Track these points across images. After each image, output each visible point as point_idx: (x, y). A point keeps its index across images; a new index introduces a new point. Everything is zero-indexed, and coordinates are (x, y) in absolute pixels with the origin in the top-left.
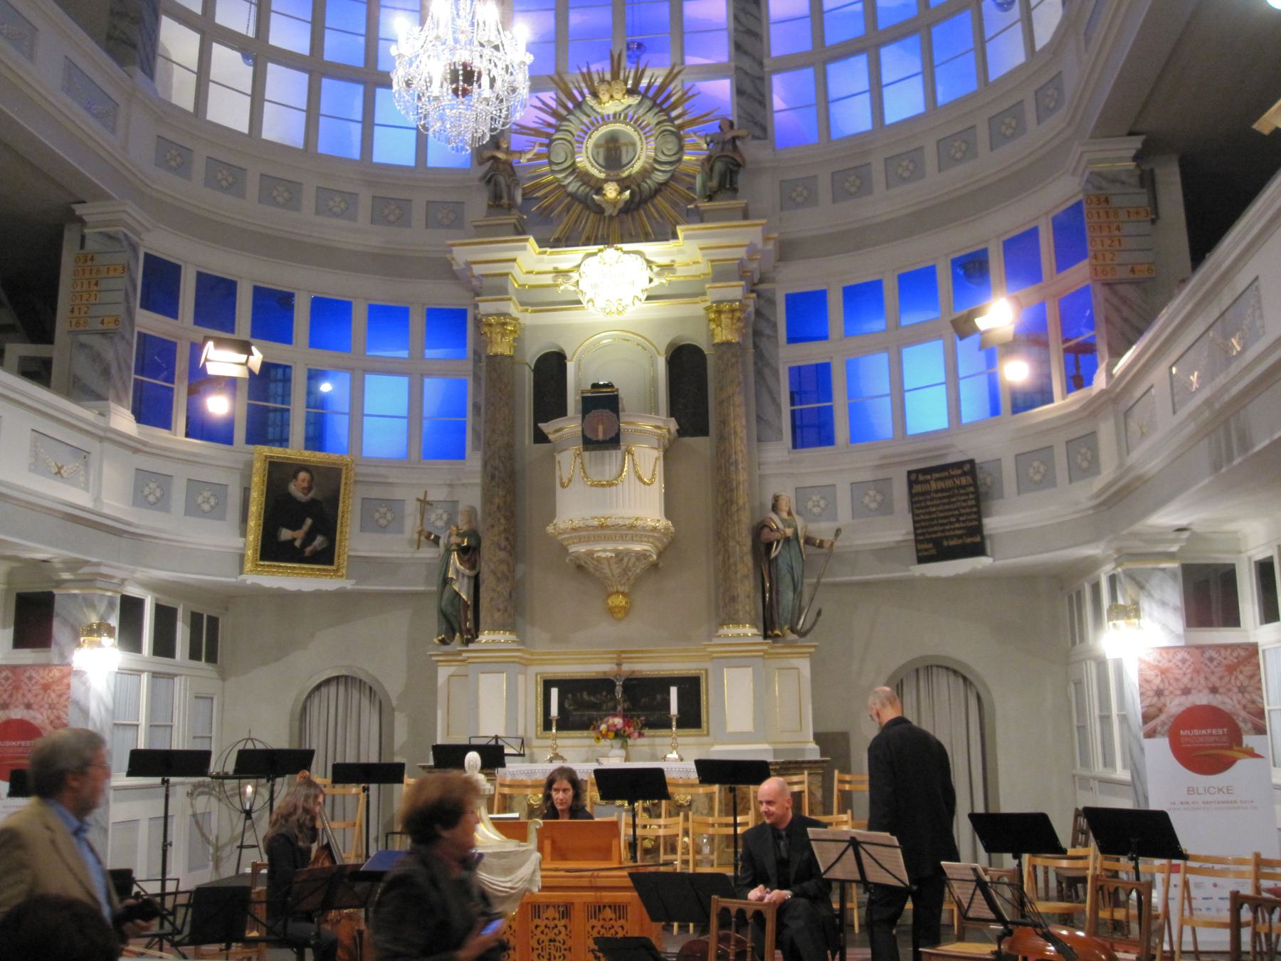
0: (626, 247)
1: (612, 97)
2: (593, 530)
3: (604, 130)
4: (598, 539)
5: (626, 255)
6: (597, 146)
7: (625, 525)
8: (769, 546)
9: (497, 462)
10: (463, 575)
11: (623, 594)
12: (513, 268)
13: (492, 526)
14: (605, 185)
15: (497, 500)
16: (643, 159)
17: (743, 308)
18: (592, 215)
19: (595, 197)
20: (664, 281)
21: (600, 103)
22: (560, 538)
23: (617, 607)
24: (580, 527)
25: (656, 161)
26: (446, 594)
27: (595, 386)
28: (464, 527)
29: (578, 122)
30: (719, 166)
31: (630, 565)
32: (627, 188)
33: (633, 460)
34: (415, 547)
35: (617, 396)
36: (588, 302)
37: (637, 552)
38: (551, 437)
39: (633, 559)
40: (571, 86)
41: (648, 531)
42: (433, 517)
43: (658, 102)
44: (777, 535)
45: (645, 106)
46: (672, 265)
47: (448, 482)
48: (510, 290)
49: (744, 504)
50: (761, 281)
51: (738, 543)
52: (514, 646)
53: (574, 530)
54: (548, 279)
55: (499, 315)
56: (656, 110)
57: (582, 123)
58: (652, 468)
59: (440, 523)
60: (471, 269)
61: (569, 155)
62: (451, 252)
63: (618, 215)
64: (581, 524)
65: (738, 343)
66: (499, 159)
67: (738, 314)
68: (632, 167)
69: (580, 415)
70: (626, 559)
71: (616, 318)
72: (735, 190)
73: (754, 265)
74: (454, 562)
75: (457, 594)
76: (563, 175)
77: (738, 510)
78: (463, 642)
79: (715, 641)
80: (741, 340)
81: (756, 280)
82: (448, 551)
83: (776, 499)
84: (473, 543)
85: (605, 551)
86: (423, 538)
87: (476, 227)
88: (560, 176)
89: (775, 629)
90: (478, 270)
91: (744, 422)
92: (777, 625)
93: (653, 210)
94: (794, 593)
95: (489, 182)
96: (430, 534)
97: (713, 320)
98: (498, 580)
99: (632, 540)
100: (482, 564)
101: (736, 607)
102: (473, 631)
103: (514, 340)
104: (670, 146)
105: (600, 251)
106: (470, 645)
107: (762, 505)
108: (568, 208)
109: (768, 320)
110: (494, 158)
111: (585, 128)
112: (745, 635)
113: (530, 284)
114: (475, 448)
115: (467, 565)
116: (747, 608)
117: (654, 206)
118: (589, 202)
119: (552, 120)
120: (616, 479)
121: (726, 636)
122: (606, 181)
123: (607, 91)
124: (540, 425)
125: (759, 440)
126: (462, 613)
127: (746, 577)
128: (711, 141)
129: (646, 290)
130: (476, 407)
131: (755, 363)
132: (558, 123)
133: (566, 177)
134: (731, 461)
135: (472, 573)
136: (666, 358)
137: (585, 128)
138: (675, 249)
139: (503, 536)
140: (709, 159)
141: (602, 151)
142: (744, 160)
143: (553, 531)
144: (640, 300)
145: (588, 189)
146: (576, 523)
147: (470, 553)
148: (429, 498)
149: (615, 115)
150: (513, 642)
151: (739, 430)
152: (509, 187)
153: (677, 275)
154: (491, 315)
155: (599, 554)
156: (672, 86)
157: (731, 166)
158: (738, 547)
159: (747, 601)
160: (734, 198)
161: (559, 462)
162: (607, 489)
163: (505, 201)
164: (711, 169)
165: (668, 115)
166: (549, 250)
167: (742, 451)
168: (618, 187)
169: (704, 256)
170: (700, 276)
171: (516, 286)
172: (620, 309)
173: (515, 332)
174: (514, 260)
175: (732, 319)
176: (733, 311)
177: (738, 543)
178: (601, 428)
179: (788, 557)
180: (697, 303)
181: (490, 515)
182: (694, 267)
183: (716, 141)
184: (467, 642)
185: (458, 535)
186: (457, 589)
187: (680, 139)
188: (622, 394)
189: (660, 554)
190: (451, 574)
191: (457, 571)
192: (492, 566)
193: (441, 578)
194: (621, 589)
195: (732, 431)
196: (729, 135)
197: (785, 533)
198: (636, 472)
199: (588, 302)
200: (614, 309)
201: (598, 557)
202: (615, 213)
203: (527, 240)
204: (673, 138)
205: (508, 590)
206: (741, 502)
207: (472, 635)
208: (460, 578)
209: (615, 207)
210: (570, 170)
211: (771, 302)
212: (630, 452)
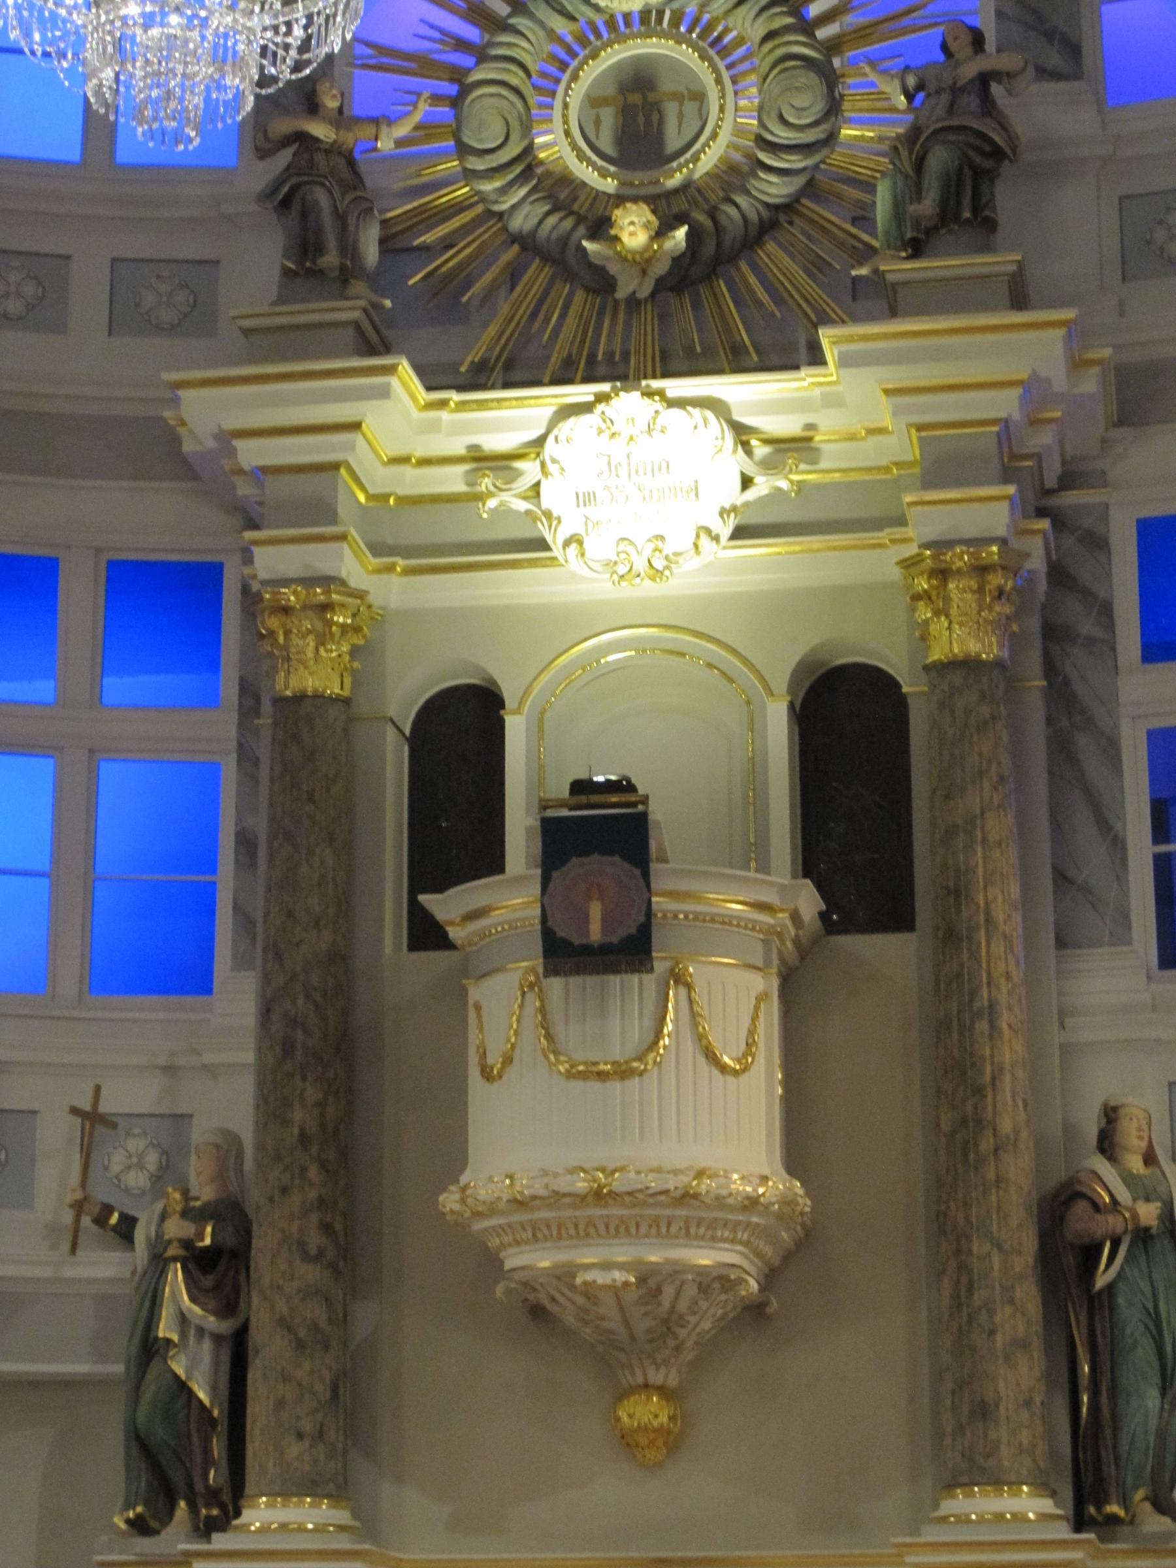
0: (676, 387)
2: (573, 1206)
3: (615, 55)
4: (586, 1232)
5: (676, 412)
6: (594, 101)
7: (666, 1192)
8: (1089, 1254)
9: (301, 1001)
10: (201, 1331)
11: (661, 1390)
12: (352, 447)
13: (284, 1190)
14: (617, 213)
15: (298, 1115)
16: (724, 137)
17: (1011, 563)
18: (579, 296)
19: (585, 243)
20: (783, 484)
22: (478, 1226)
23: (643, 1429)
24: (534, 1198)
26: (149, 1392)
27: (581, 787)
28: (205, 1193)
29: (541, 33)
30: (939, 159)
31: (683, 1305)
32: (680, 219)
33: (691, 1001)
34: (65, 1246)
35: (642, 818)
36: (567, 543)
37: (701, 1271)
38: (454, 933)
39: (691, 1291)
41: (731, 1209)
42: (118, 1161)
44: (1114, 1223)
46: (809, 439)
47: (162, 1060)
48: (342, 510)
49: (1016, 1131)
50: (1068, 481)
51: (998, 1246)
52: (344, 1543)
53: (519, 1203)
54: (452, 480)
55: (309, 582)
57: (552, 35)
58: (746, 1023)
59: (137, 1180)
60: (233, 452)
61: (515, 125)
62: (176, 402)
63: (653, 295)
64: (539, 1189)
65: (998, 664)
66: (317, 140)
67: (996, 580)
68: (696, 159)
69: (539, 871)
70: (669, 1292)
71: (647, 588)
72: (990, 225)
73: (1044, 438)
74: (175, 1297)
75: (182, 1387)
76: (498, 184)
77: (996, 1150)
78: (196, 1529)
79: (931, 1534)
80: (1006, 654)
81: (1051, 481)
82: (159, 1262)
83: (1111, 1114)
84: (230, 1240)
85: (606, 1266)
86: (86, 1221)
87: (247, 332)
88: (488, 187)
89: (1107, 1501)
90: (251, 453)
91: (1015, 890)
92: (1113, 1490)
93: (752, 280)
94: (1163, 1394)
95: (285, 204)
96: (108, 1209)
97: (926, 596)
98: (300, 1345)
99: (688, 1233)
100: (255, 1300)
101: (993, 1435)
102: (226, 1497)
103: (354, 652)
104: (802, 100)
105: (602, 398)
106: (215, 1536)
107: (1070, 1130)
108: (514, 275)
109: (1087, 594)
110: (302, 139)
111: (561, 53)
112: (1019, 1518)
113: (401, 492)
114: (241, 962)
115: (212, 1304)
116: (1025, 1437)
117: (755, 268)
118: (572, 260)
119: (470, 32)
120: (640, 1058)
121: (963, 1520)
122: (620, 199)
124: (422, 898)
125: (1061, 943)
126: (195, 1439)
127: (1022, 1344)
128: (920, 87)
129: (734, 509)
130: (245, 842)
131: (1049, 721)
132: (487, 37)
133: (504, 191)
134: (977, 1005)
135: (225, 1327)
136: (791, 705)
137: (561, 53)
138: (817, 392)
139: (314, 1218)
140: (914, 134)
141: (608, 116)
142: (1012, 139)
143: (457, 1207)
144: (716, 539)
145: (568, 223)
146: (526, 1185)
147: (221, 1267)
148: (105, 1107)
149: (645, 14)
150: (341, 1528)
151: (999, 915)
152: (341, 218)
153: (823, 465)
154: (286, 582)
155: (589, 1276)
157: (978, 160)
158: (996, 1260)
159: (1025, 1414)
160: (987, 248)
161: (478, 1008)
162: (616, 1086)
163: (331, 259)
164: (919, 166)
165: (796, 12)
166: (455, 397)
167: (1008, 976)
168: (652, 218)
169: (896, 412)
170: (887, 469)
171: (362, 498)
172: (659, 564)
173: (357, 629)
174: (356, 426)
175: (981, 591)
176: (982, 570)
177: (998, 1246)
178: (595, 911)
179: (1147, 1290)
180: (882, 546)
181: (278, 1158)
182: (872, 441)
183: (932, 87)
184: (207, 1528)
185: (186, 1214)
186: (181, 1372)
187: (830, 79)
188: (657, 812)
189: (771, 1277)
190: (165, 1329)
191: (183, 1320)
192: (282, 1307)
193: (139, 1333)
194: (656, 1377)
195: (982, 918)
196: (969, 71)
197: (1135, 1216)
198: (700, 1038)
199: (567, 543)
200: (640, 565)
201: (586, 1283)
202: (645, 292)
203: (391, 370)
204: (810, 79)
205: (327, 1376)
206: (1006, 1125)
207: (223, 1507)
208: (192, 1340)
209: (644, 272)
210: (518, 170)
211: (1098, 543)
212: (679, 978)
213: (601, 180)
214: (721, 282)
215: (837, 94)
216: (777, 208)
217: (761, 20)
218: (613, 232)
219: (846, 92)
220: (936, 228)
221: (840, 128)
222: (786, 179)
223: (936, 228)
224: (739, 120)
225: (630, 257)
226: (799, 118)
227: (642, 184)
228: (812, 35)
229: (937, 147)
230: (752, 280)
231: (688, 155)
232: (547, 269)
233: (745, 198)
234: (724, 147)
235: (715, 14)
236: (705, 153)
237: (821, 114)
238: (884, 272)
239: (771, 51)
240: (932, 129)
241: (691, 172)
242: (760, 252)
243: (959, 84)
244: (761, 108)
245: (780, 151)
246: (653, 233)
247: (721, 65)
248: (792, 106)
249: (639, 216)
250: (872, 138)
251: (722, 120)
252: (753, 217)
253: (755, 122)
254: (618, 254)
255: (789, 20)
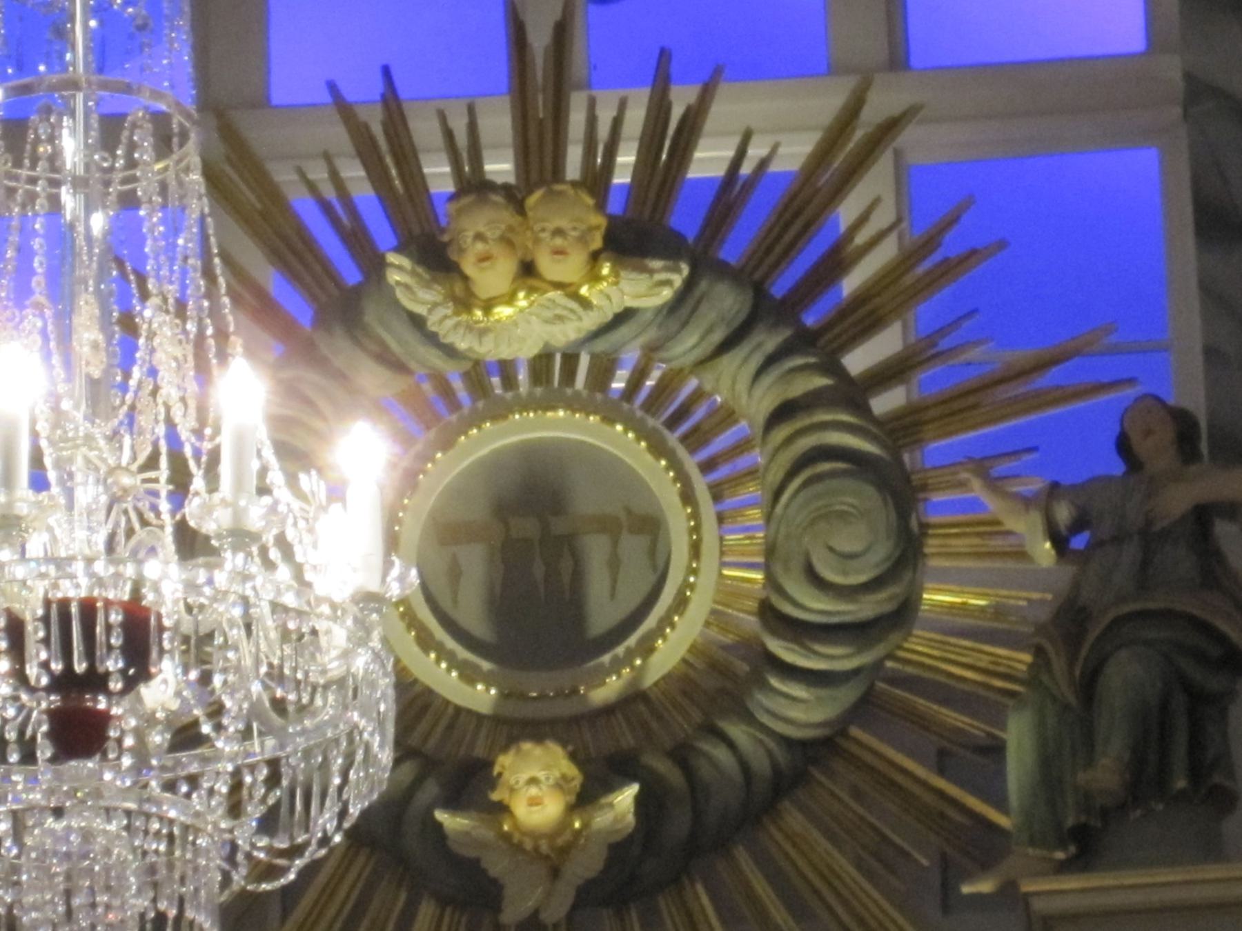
1: (528, 270)
19: (441, 816)
21: (465, 301)
25: (770, 615)
40: (284, 176)
43: (779, 288)
45: (708, 314)
56: (768, 340)
68: (646, 648)
93: (761, 887)
117: (764, 862)
123: (507, 241)
128: (1079, 524)
149: (541, 365)
156: (846, 212)
157: (1196, 674)
164: (1089, 686)
168: (571, 770)
202: (557, 911)
209: (555, 873)
213: (466, 688)
214: (700, 888)
215: (914, 524)
216: (802, 745)
217: (767, 380)
218: (495, 796)
219: (934, 519)
220: (1122, 807)
221: (921, 590)
222: (823, 692)
223: (1122, 807)
224: (726, 572)
225: (528, 845)
226: (845, 573)
227: (542, 697)
228: (862, 408)
229: (1124, 654)
230: (761, 887)
231: (632, 641)
232: (361, 860)
233: (744, 727)
234: (699, 627)
235: (676, 364)
236: (665, 638)
237: (887, 565)
238: (1027, 895)
239: (789, 440)
240: (1111, 615)
241: (639, 673)
242: (773, 830)
243: (1157, 527)
244: (770, 550)
245: (816, 639)
246: (572, 798)
247: (691, 463)
248: (831, 549)
249: (547, 767)
250: (982, 609)
251: (695, 572)
252: (760, 763)
253: (758, 576)
254: (506, 837)
255: (820, 381)
